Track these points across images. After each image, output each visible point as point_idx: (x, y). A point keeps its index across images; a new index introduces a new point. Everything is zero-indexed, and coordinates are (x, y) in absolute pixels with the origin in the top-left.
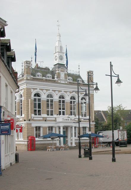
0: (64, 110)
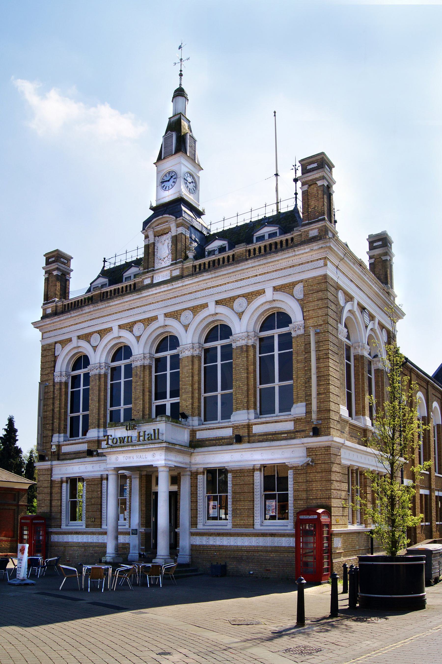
0: (176, 400)
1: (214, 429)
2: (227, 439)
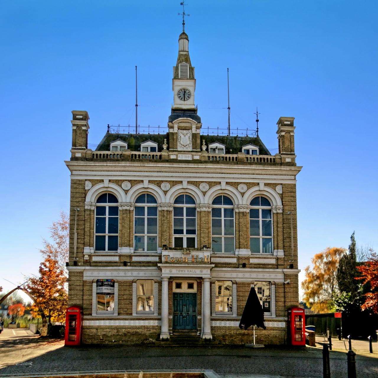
1: (224, 257)
2: (233, 264)
